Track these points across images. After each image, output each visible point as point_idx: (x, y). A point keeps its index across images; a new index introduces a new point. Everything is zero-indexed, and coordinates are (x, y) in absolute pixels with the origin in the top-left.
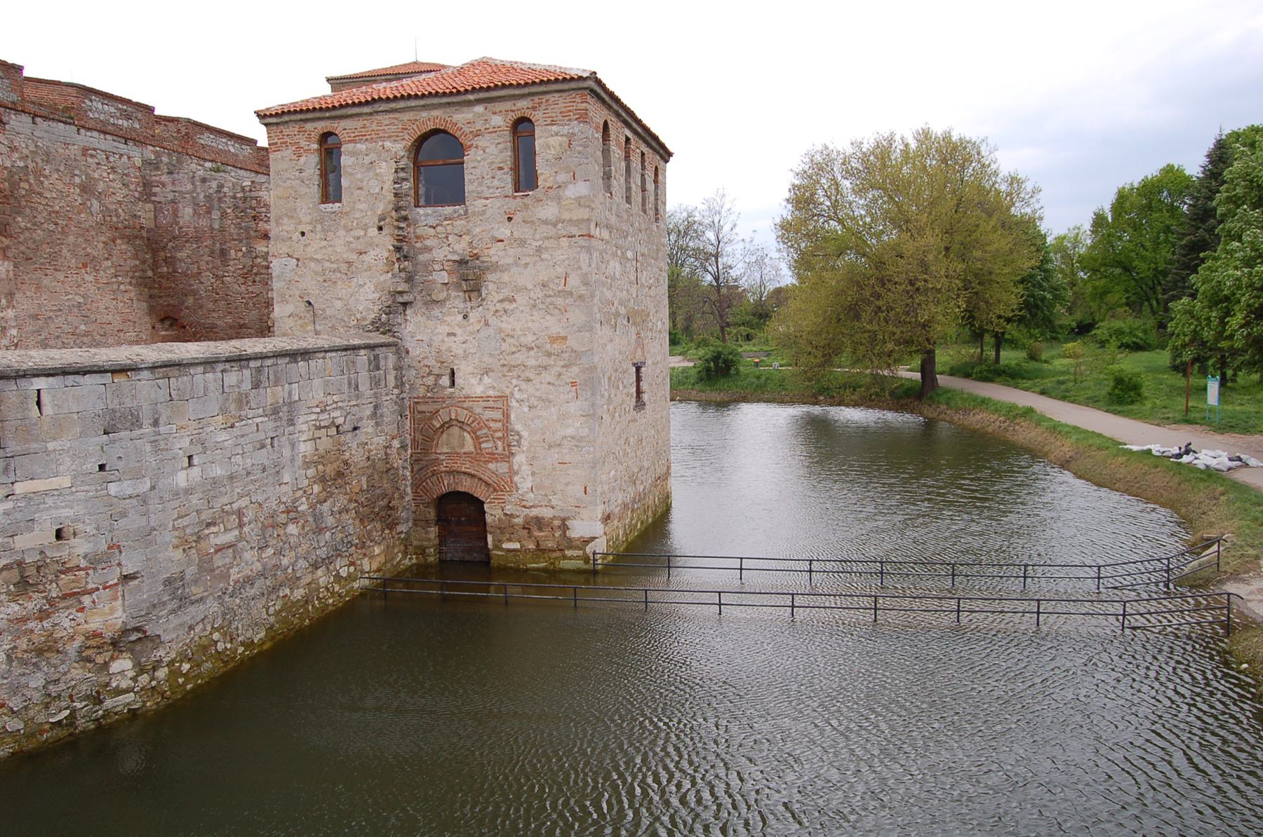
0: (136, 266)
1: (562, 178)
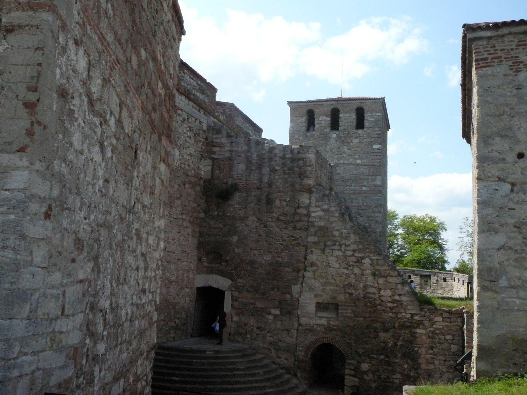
0: (194, 208)
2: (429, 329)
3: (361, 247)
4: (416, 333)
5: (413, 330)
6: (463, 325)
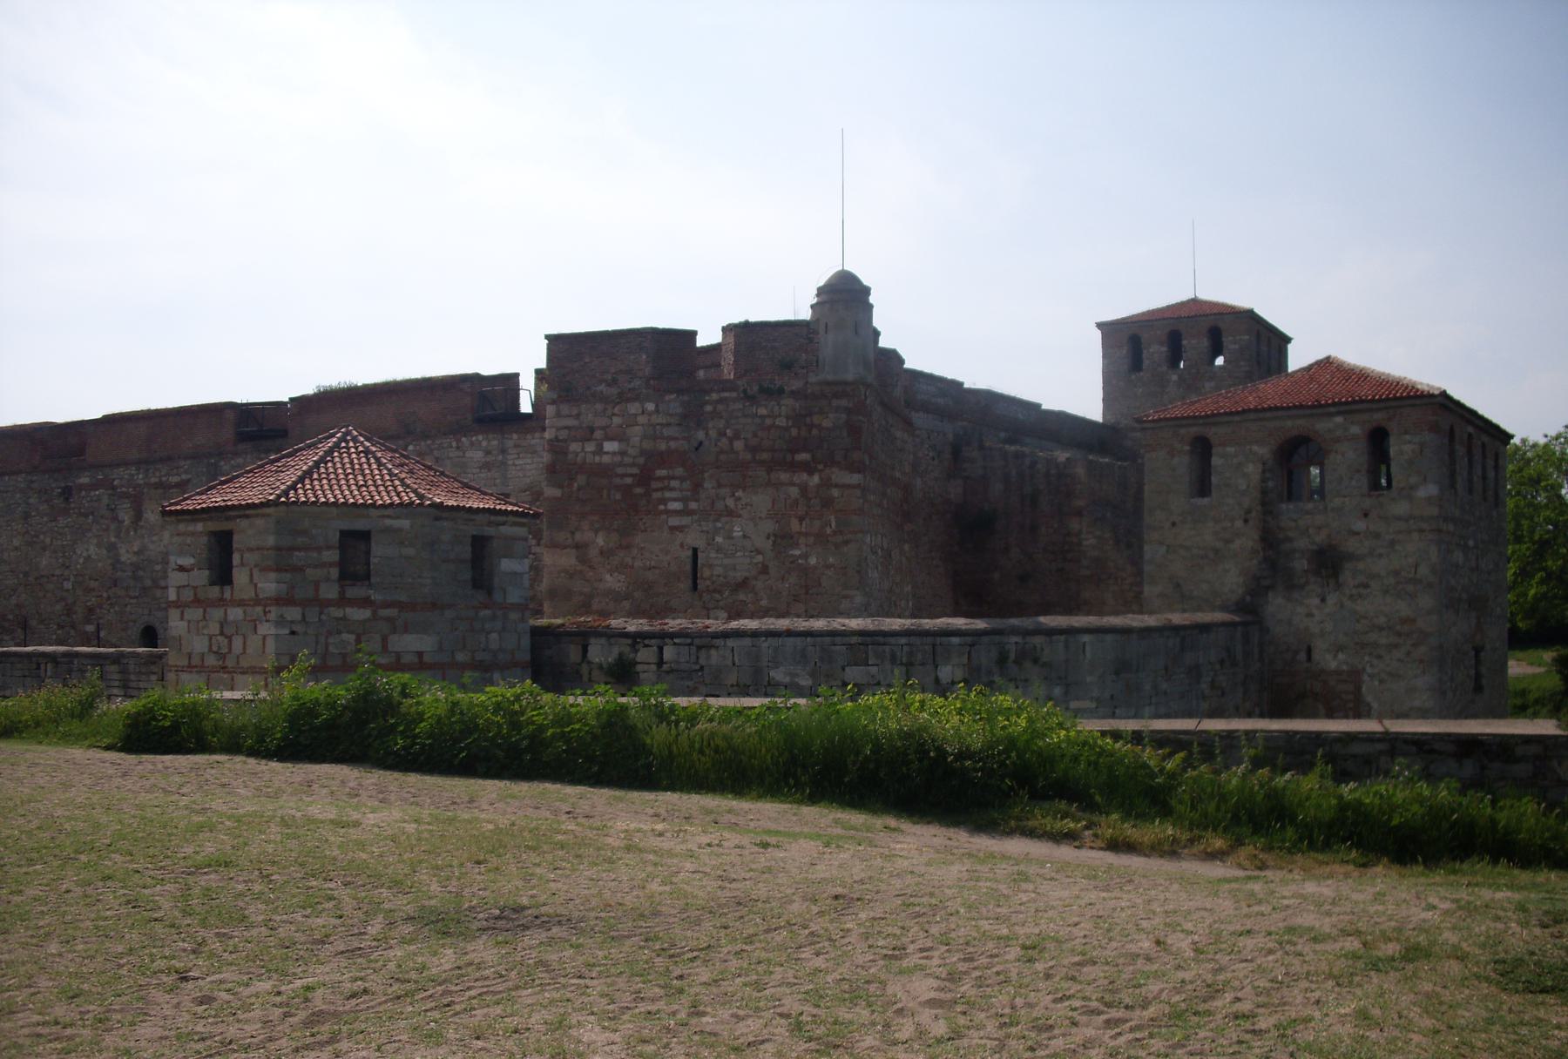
1: (1413, 480)
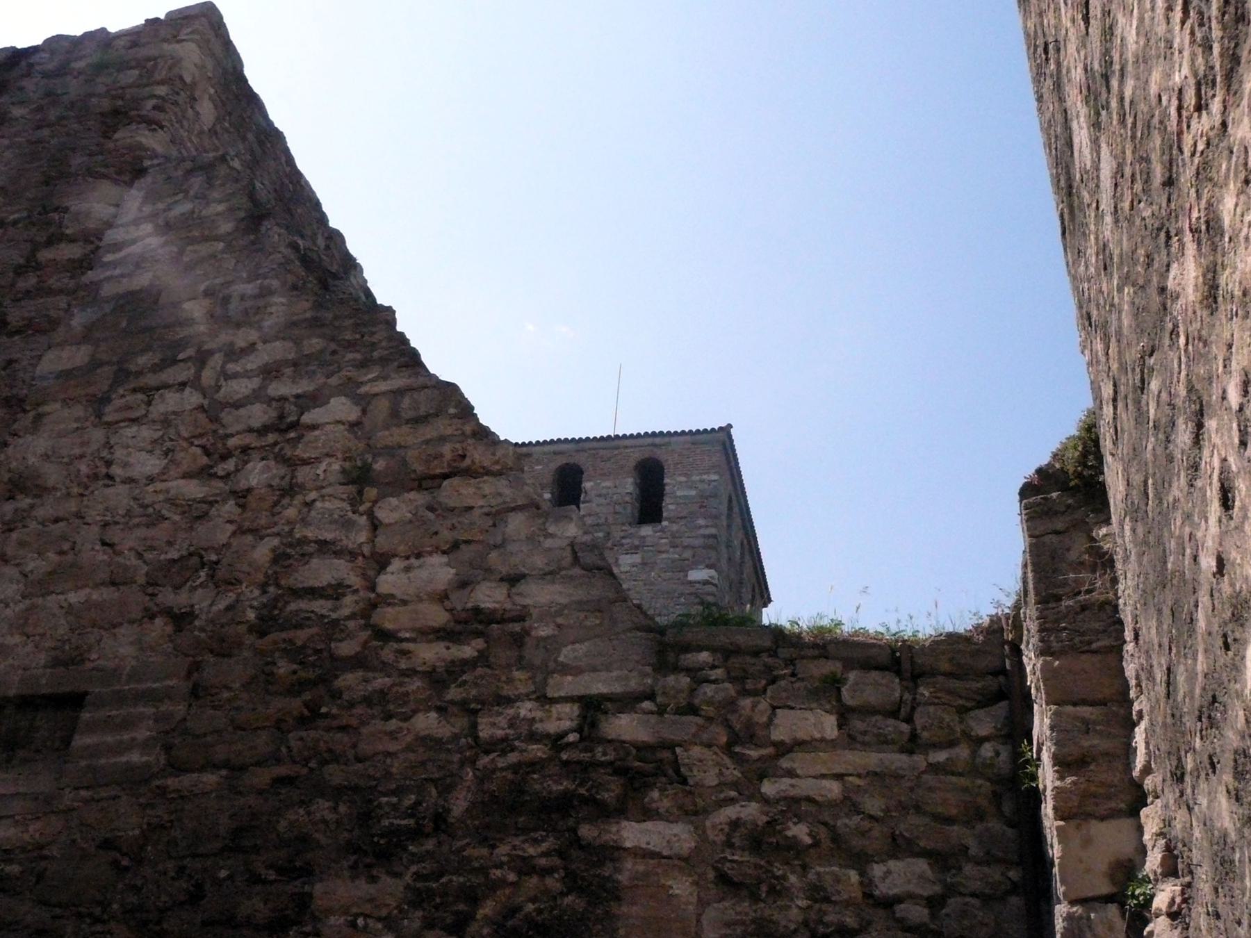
2: (730, 812)
3: (315, 344)
4: (614, 852)
5: (587, 832)
6: (1019, 730)
